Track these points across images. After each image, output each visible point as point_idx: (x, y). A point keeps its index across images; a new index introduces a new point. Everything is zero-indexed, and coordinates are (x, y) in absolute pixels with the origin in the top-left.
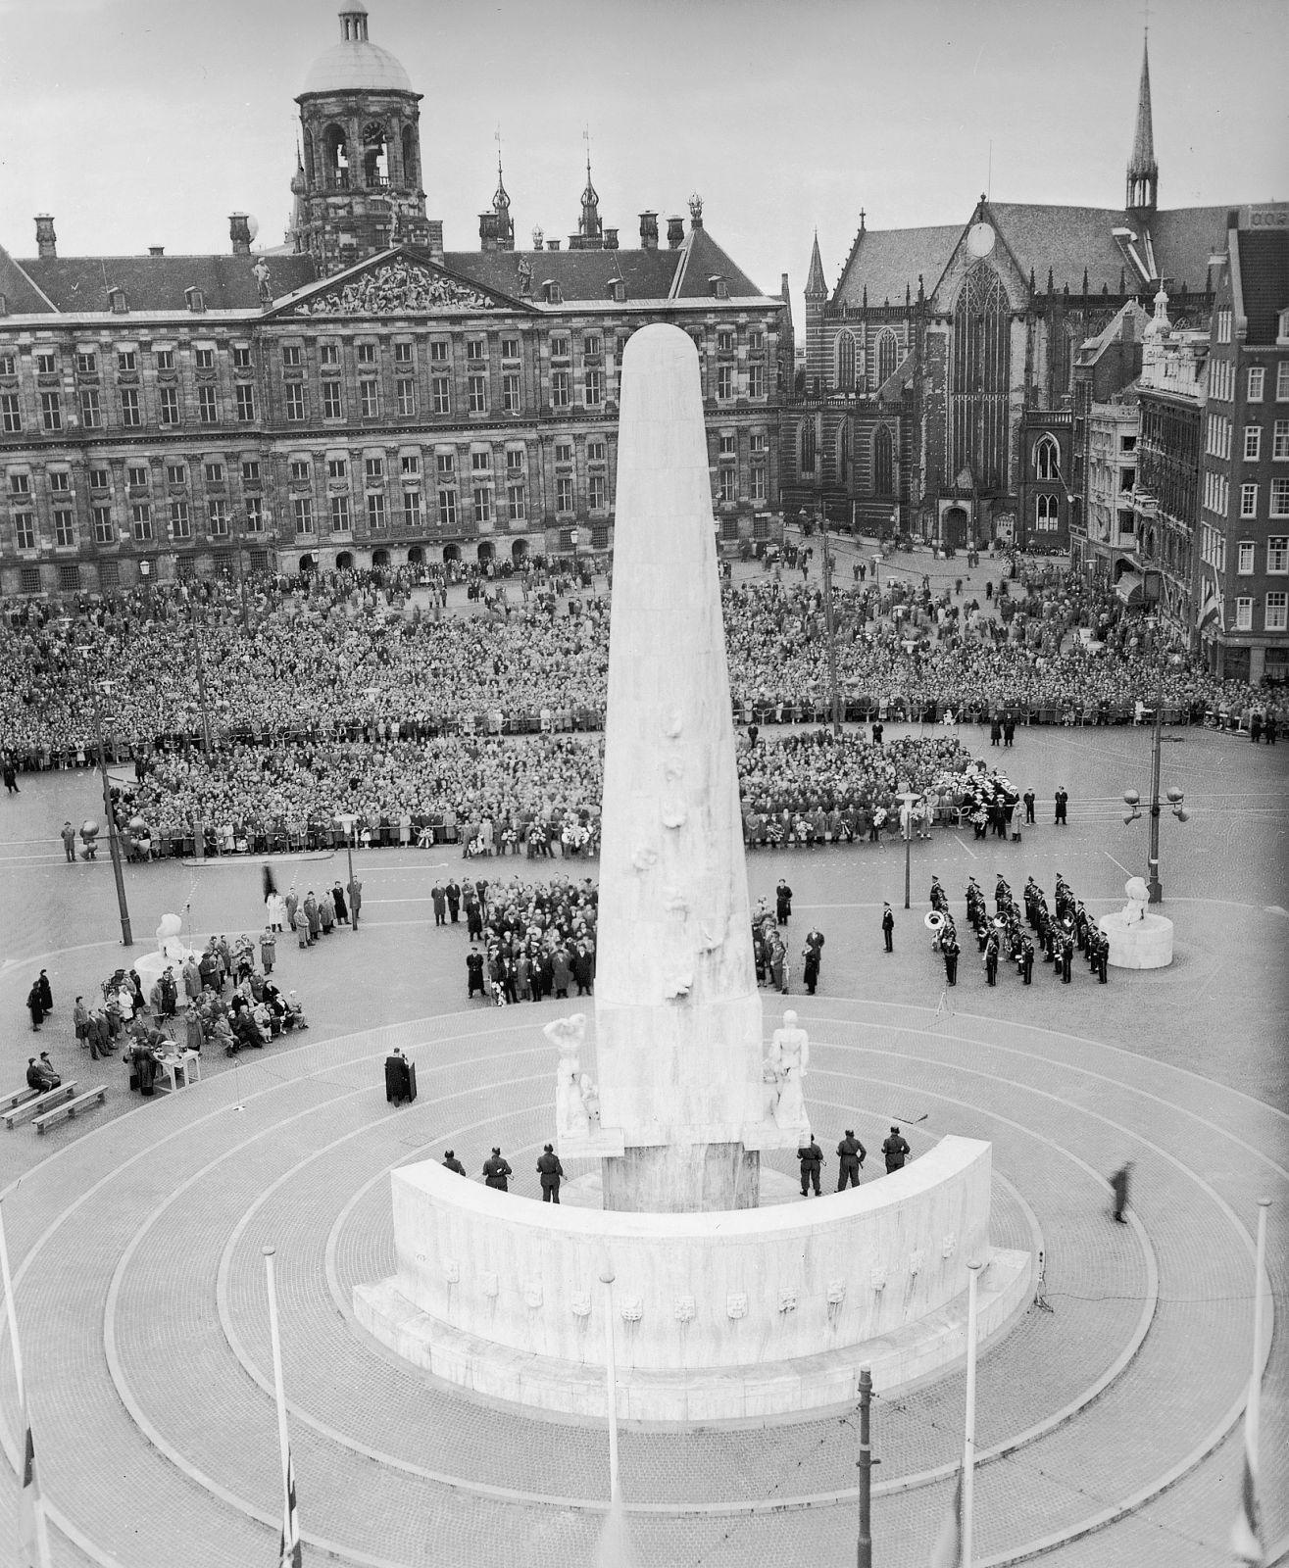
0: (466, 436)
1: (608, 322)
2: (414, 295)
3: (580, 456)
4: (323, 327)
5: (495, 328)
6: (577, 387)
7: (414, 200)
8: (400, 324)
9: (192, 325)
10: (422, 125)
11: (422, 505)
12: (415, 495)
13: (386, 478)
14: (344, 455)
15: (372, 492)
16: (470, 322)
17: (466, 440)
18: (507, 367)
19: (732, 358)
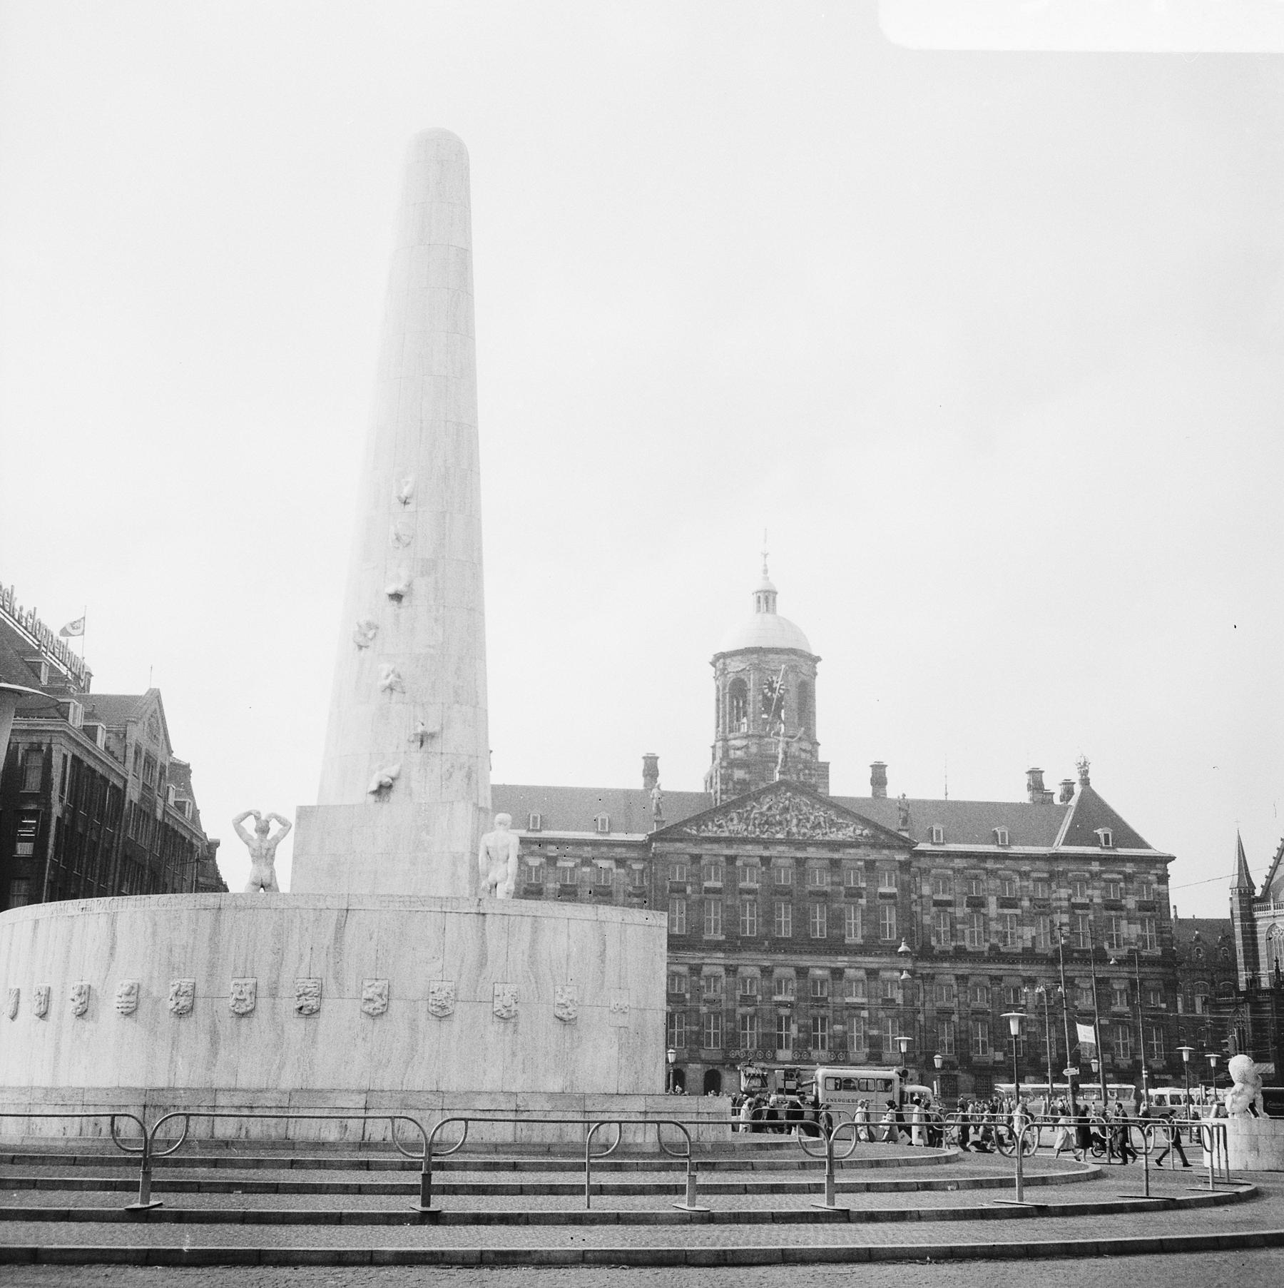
0: (841, 961)
1: (989, 865)
2: (795, 821)
4: (708, 846)
5: (872, 857)
6: (959, 927)
7: (805, 745)
9: (594, 844)
11: (794, 1028)
12: (788, 1018)
13: (759, 998)
14: (721, 971)
15: (741, 1010)
17: (840, 965)
18: (883, 896)
19: (1121, 908)
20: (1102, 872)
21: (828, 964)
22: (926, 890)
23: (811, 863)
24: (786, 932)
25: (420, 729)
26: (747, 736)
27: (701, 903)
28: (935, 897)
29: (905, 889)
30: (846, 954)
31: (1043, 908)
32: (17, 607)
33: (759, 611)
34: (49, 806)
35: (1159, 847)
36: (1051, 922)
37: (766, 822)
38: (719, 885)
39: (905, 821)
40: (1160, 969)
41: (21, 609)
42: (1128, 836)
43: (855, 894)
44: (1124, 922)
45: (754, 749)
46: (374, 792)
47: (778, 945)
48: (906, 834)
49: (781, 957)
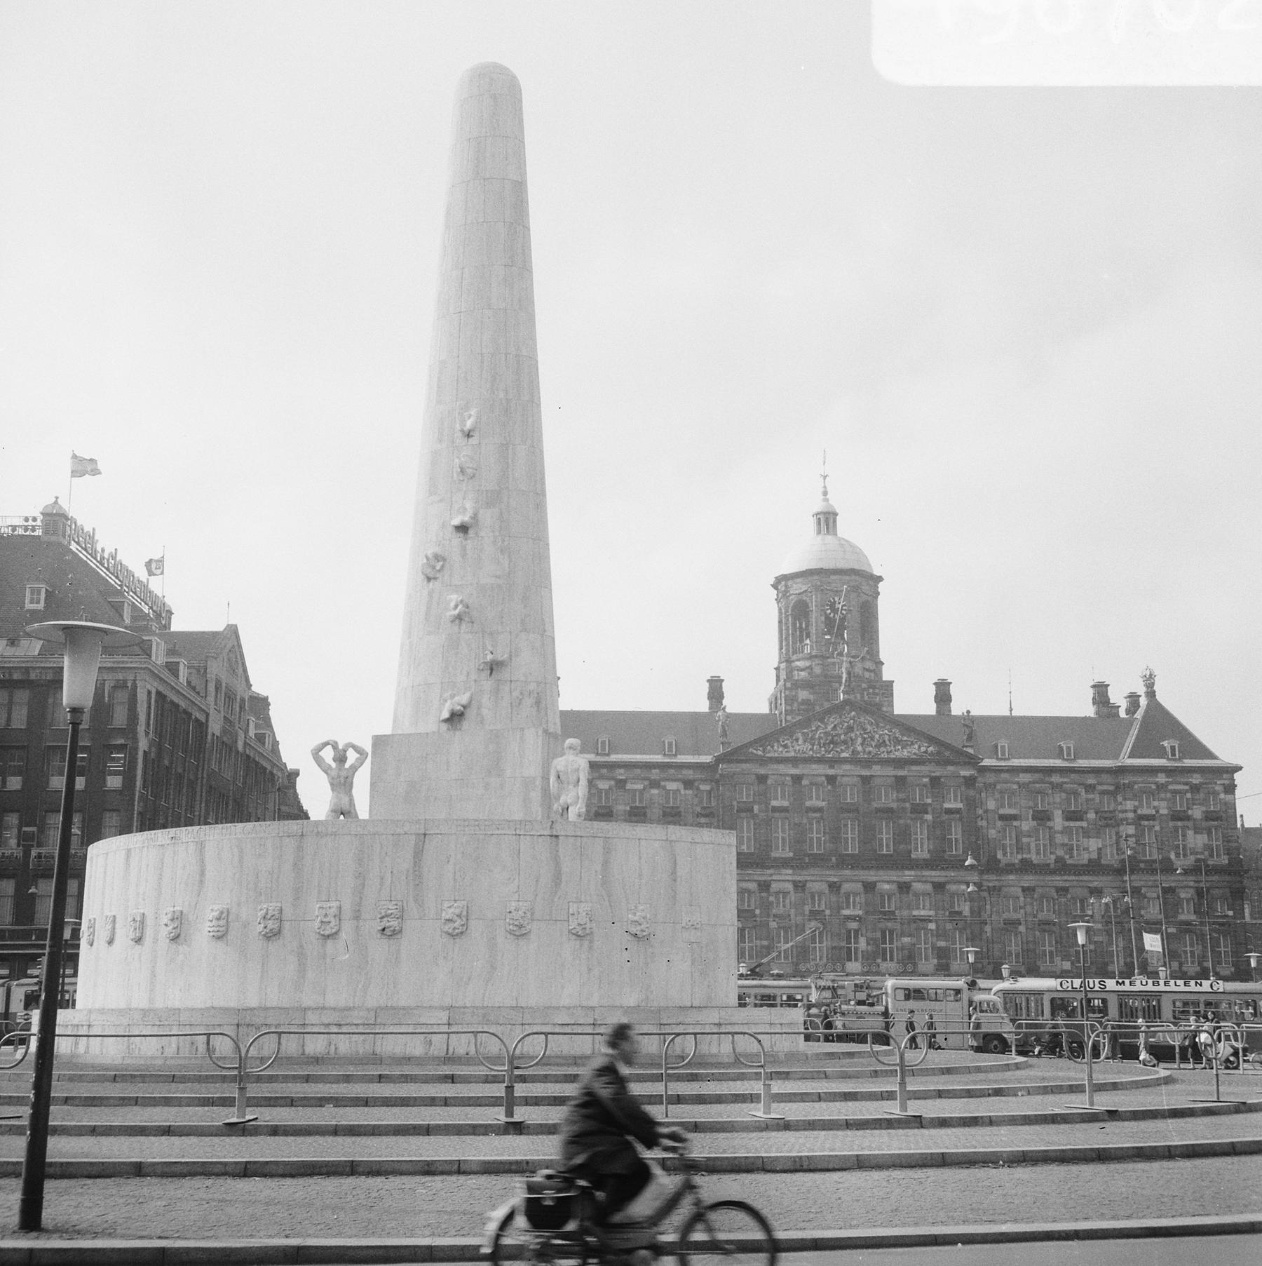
0: (908, 875)
1: (1056, 779)
2: (860, 740)
3: (1028, 909)
4: (775, 766)
5: (938, 774)
6: (1025, 840)
7: (869, 665)
8: (848, 767)
10: (881, 601)
11: (862, 941)
12: (856, 931)
14: (790, 887)
16: (914, 768)
17: (907, 879)
18: (949, 811)
19: (1188, 818)
20: (1168, 783)
21: (895, 878)
22: (991, 805)
23: (878, 781)
24: (852, 848)
25: (489, 657)
26: (811, 657)
27: (768, 822)
28: (1002, 812)
29: (972, 804)
30: (912, 869)
31: (1109, 821)
32: (99, 549)
33: (819, 532)
34: (135, 739)
35: (1225, 755)
36: (1117, 833)
37: (832, 742)
38: (786, 803)
39: (970, 738)
40: (1227, 878)
41: (103, 550)
42: (1193, 746)
43: (920, 810)
44: (1190, 833)
45: (817, 670)
46: (446, 721)
47: (845, 862)
48: (971, 751)
49: (847, 872)
